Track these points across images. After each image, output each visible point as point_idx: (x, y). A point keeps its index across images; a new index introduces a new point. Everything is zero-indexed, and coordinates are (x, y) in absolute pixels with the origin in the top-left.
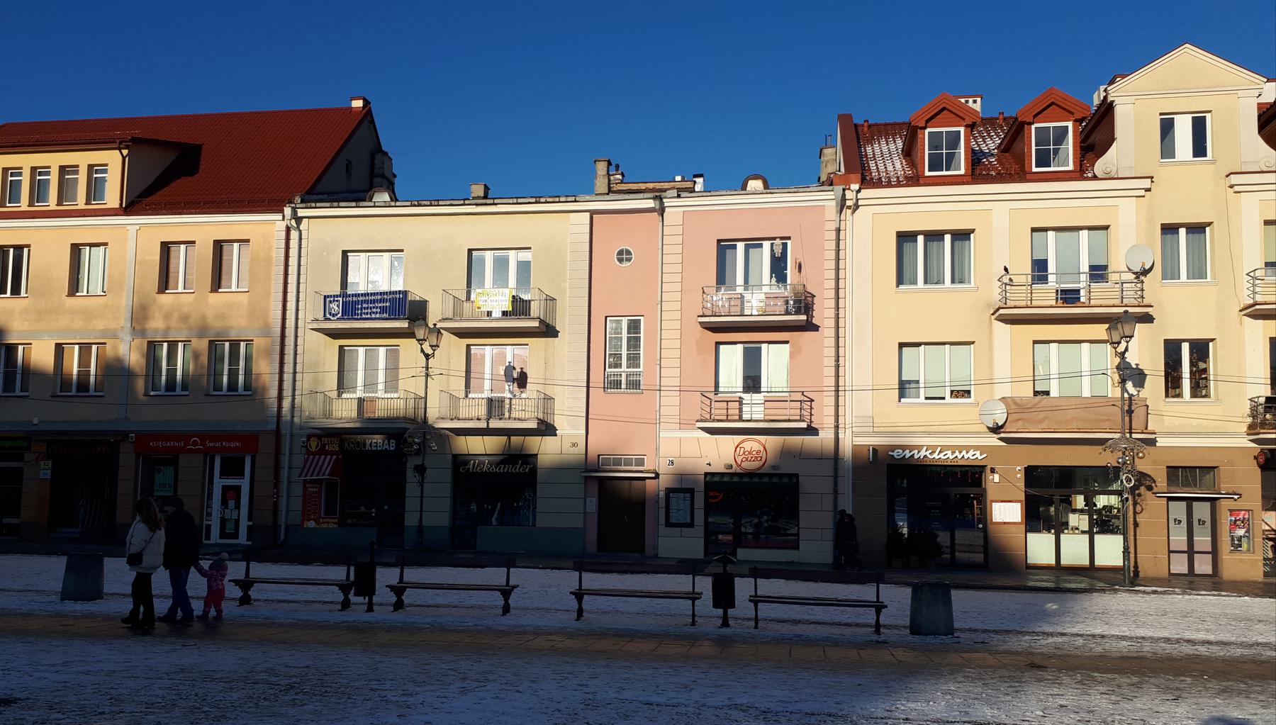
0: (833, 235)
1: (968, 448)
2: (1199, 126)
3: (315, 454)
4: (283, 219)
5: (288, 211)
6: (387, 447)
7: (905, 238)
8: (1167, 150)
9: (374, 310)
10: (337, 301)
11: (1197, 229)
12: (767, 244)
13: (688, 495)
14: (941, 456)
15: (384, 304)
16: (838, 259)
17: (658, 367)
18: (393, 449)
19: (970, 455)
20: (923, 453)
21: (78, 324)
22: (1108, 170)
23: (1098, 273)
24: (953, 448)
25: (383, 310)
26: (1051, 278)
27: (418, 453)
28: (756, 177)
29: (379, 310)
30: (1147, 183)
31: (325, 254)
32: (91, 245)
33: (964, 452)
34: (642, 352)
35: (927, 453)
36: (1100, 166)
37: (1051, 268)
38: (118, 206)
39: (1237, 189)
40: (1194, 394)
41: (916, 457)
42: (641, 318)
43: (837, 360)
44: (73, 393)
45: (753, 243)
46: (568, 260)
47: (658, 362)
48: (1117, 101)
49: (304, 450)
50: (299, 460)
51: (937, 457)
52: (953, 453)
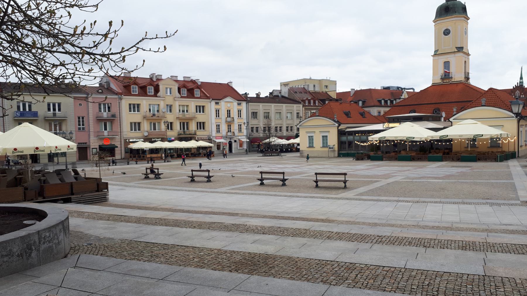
0: (118, 103)
2: (170, 89)
8: (167, 93)
23: (158, 111)
28: (100, 90)
36: (158, 95)
40: (171, 130)
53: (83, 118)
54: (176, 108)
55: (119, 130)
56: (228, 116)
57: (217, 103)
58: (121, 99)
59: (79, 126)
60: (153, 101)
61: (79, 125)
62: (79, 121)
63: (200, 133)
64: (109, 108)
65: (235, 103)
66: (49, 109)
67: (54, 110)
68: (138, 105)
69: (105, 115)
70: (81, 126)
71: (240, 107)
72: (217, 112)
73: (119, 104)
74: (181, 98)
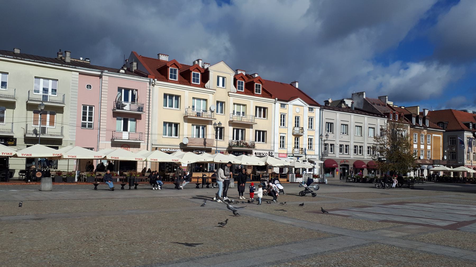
0: (148, 91)
8: (218, 84)
11: (222, 103)
14: (172, 151)
17: (99, 122)
20: (168, 150)
26: (195, 110)
33: (177, 150)
35: (169, 150)
36: (207, 85)
37: (195, 108)
39: (230, 95)
47: (99, 120)
48: (210, 71)
53: (91, 108)
54: (230, 108)
56: (295, 125)
57: (283, 106)
59: (83, 120)
60: (199, 93)
61: (84, 119)
62: (84, 113)
63: (259, 145)
64: (133, 96)
65: (307, 107)
69: (128, 107)
70: (87, 121)
71: (311, 114)
72: (283, 117)
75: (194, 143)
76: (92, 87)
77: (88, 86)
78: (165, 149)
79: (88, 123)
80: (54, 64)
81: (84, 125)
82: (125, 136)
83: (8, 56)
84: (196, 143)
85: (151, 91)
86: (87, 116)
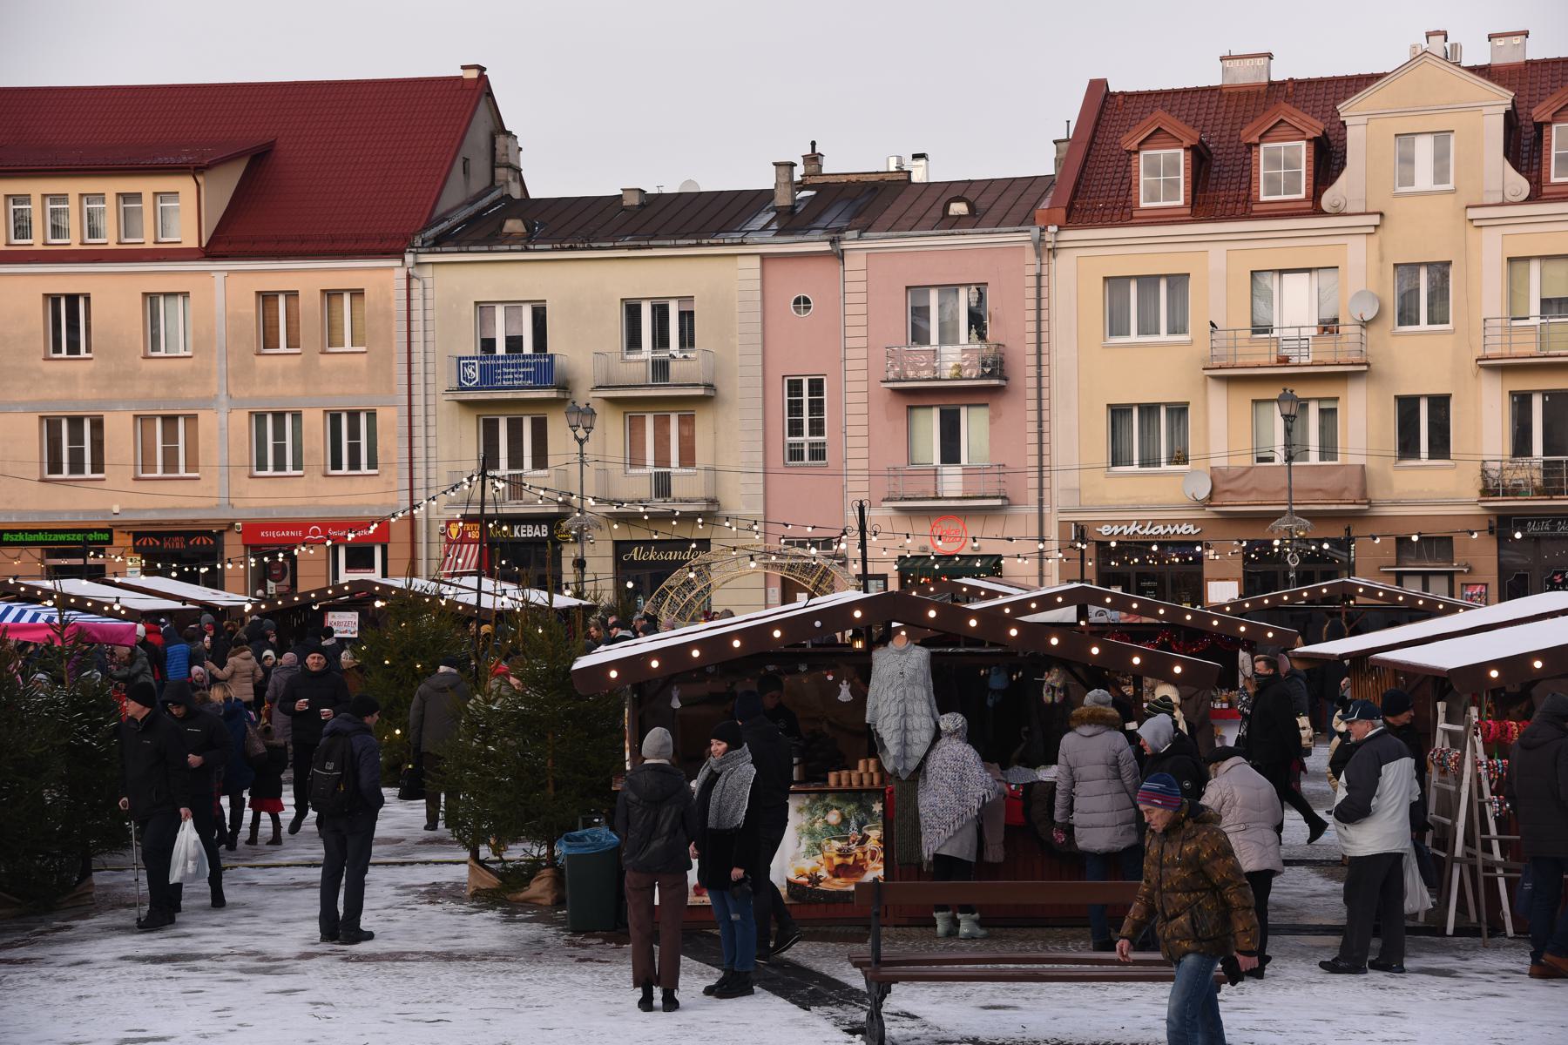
1: (1180, 522)
3: (455, 542)
4: (403, 266)
5: (409, 258)
6: (538, 533)
7: (1115, 284)
9: (516, 376)
10: (474, 364)
12: (963, 293)
13: (881, 582)
14: (1152, 531)
15: (528, 370)
16: (1039, 309)
18: (545, 535)
19: (1183, 530)
20: (1133, 528)
21: (160, 391)
22: (1336, 203)
24: (1165, 523)
25: (527, 376)
27: (577, 539)
29: (522, 376)
30: (1376, 220)
31: (454, 306)
32: (166, 295)
33: (1177, 527)
34: (825, 417)
35: (1137, 529)
36: (1327, 200)
38: (195, 245)
39: (1476, 223)
40: (1433, 455)
41: (1125, 533)
42: (824, 377)
43: (1040, 426)
44: (159, 473)
45: (949, 289)
46: (737, 310)
49: (443, 539)
50: (437, 550)
51: (1148, 533)
52: (1165, 528)
53: (817, 387)
55: (1034, 461)
58: (1054, 251)
61: (796, 429)
62: (817, 407)
66: (634, 342)
67: (661, 340)
68: (1178, 282)
70: (806, 438)
73: (1039, 287)
74: (1535, 196)
75: (1249, 492)
76: (812, 305)
77: (797, 301)
78: (1116, 527)
79: (811, 445)
80: (673, 242)
81: (796, 454)
82: (952, 482)
83: (537, 247)
84: (1253, 489)
85: (1044, 281)
86: (806, 418)
